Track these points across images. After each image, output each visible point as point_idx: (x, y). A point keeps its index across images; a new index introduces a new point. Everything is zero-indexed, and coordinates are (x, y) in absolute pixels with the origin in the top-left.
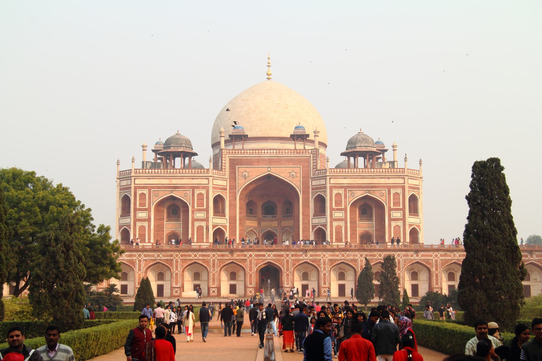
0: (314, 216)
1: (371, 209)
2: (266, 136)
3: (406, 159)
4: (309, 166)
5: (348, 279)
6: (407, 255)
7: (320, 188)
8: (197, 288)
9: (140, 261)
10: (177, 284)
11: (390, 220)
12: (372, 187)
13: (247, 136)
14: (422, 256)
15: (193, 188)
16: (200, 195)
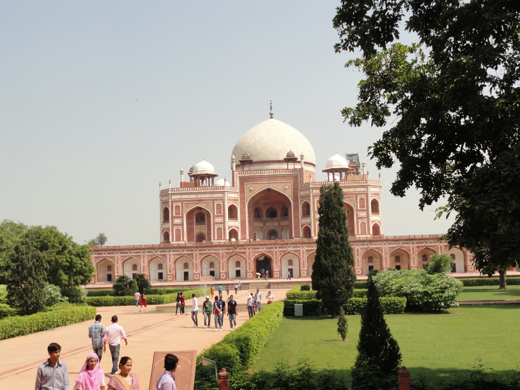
0: (302, 217)
2: (268, 160)
4: (297, 181)
6: (364, 245)
7: (306, 197)
8: (212, 273)
9: (170, 255)
10: (196, 271)
11: (358, 218)
14: (375, 245)
15: (213, 200)
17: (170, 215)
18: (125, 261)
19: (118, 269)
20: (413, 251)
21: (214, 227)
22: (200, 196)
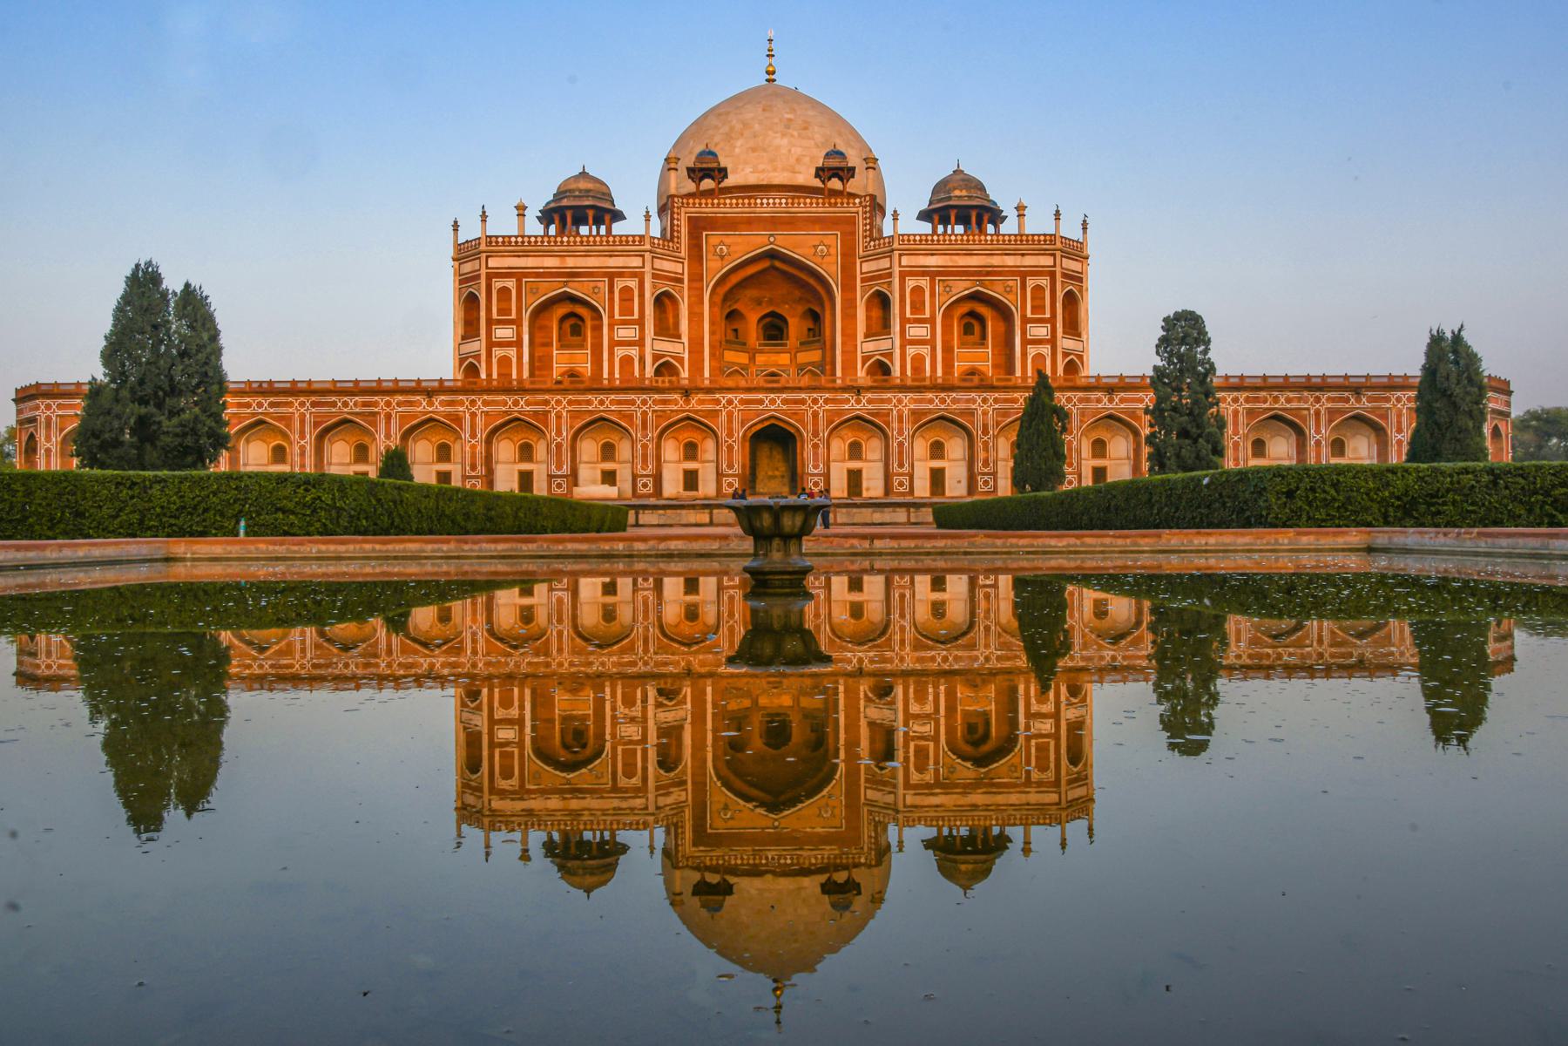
0: (866, 336)
1: (981, 320)
3: (1057, 215)
4: (853, 233)
5: (952, 456)
6: (1088, 400)
7: (880, 277)
8: (609, 478)
9: (473, 415)
10: (559, 467)
11: (1026, 342)
12: (988, 273)
13: (723, 172)
14: (1122, 400)
15: (612, 276)
16: (626, 290)
17: (483, 314)
18: (327, 430)
19: (302, 454)
20: (1236, 424)
21: (611, 354)
22: (570, 262)
